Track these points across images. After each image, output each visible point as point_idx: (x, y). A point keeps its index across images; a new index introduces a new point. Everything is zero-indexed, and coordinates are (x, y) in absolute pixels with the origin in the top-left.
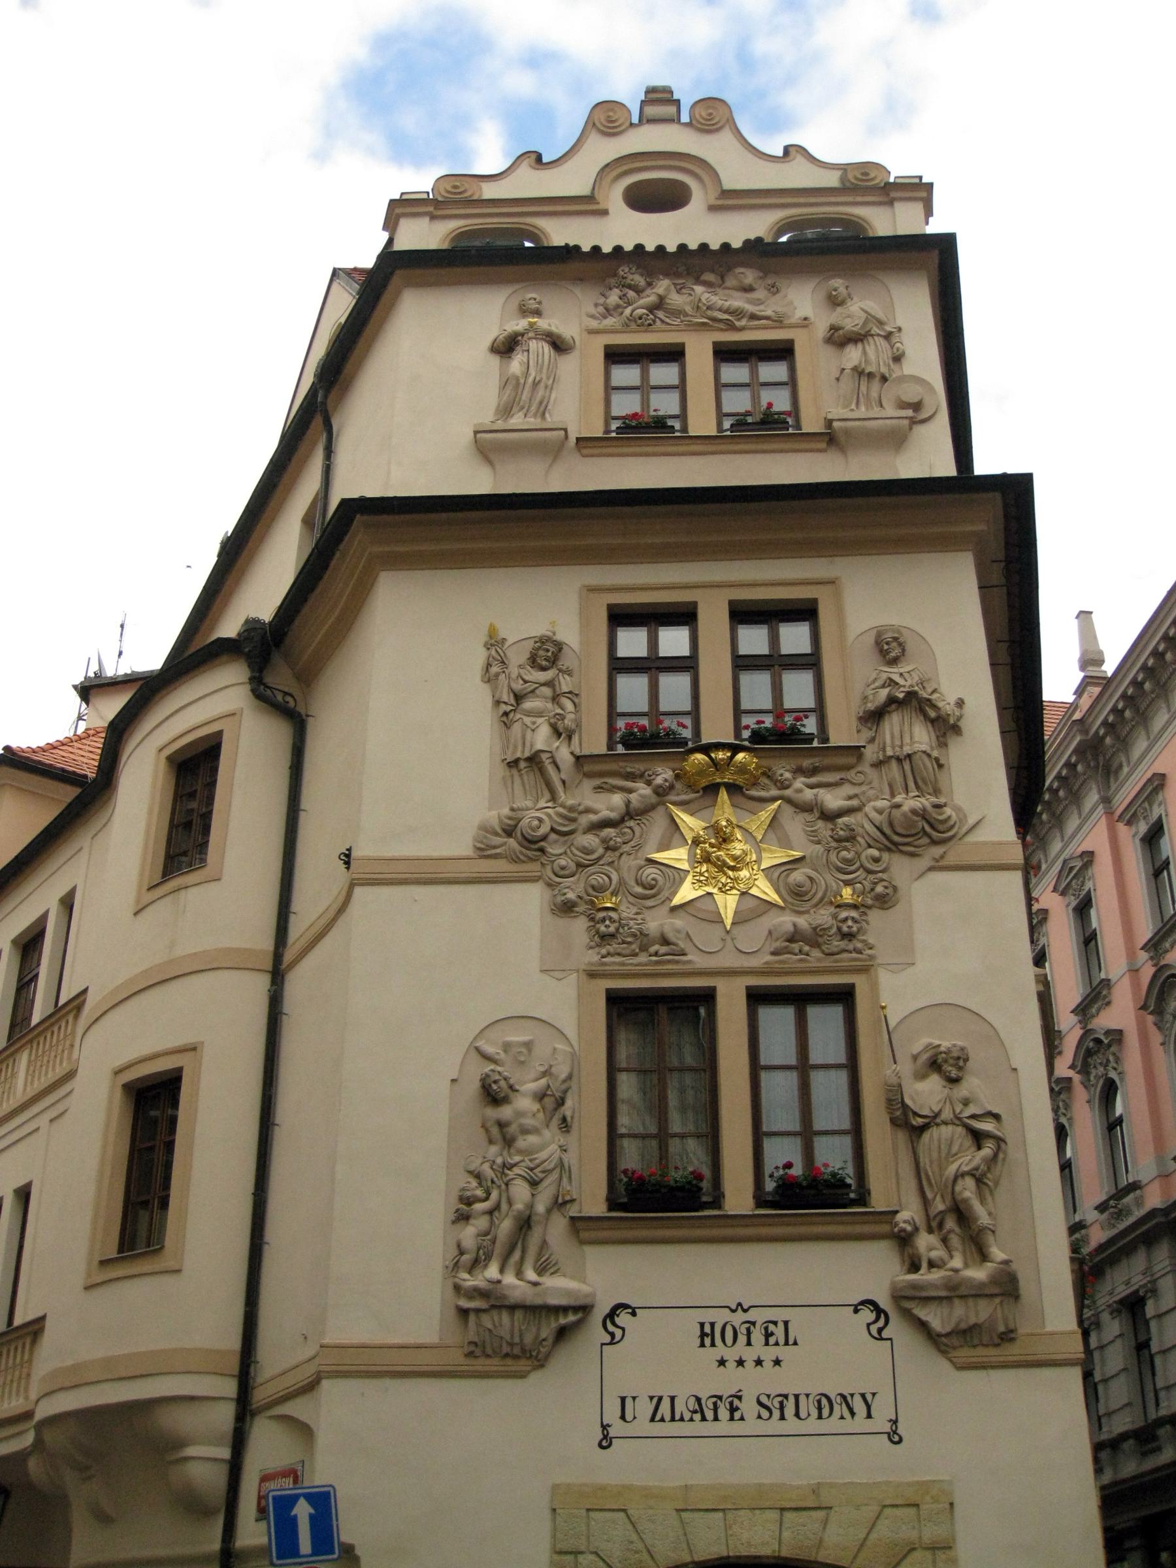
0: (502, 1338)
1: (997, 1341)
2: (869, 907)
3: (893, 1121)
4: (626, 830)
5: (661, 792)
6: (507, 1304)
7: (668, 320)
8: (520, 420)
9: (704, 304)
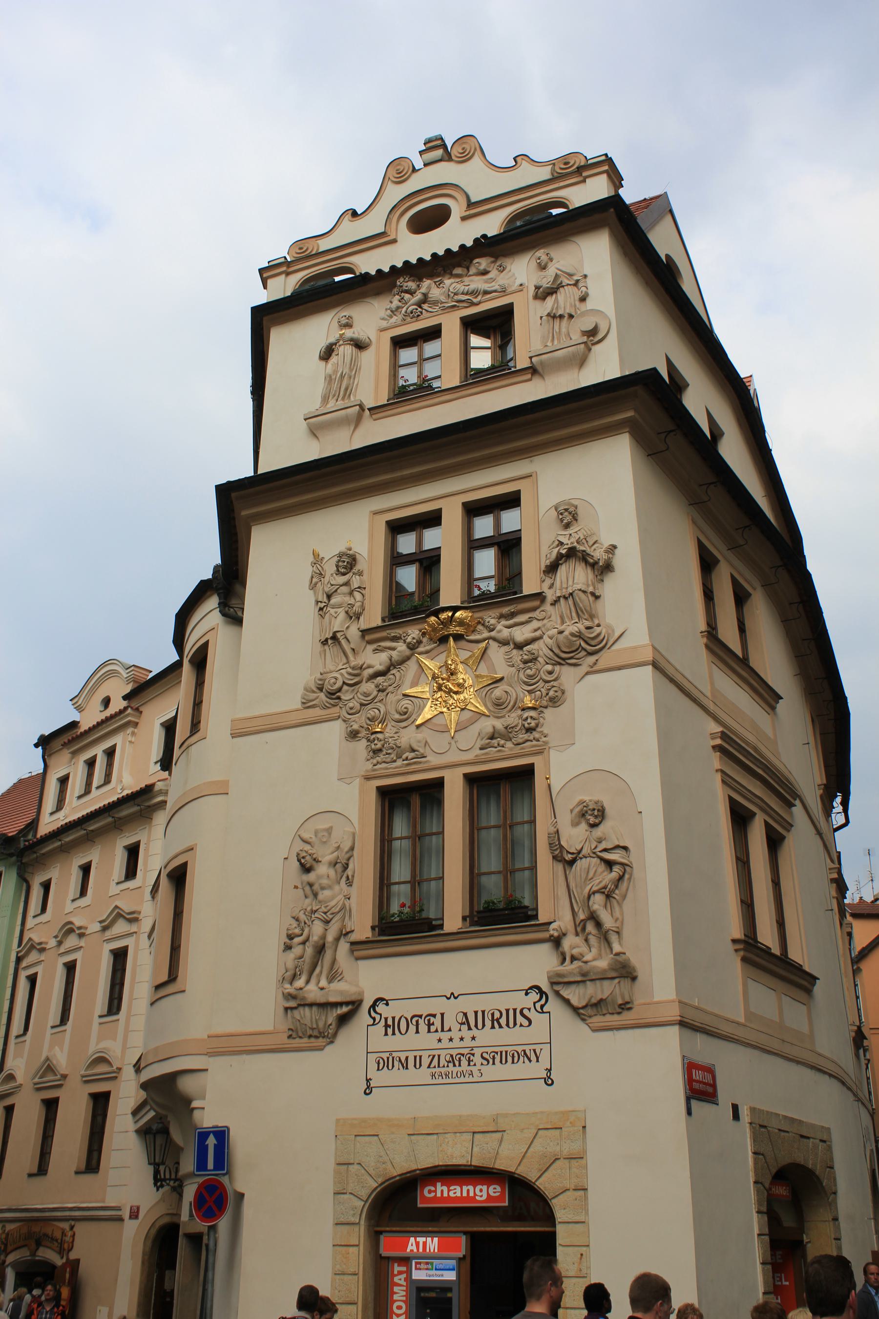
0: (306, 1025)
1: (620, 1010)
2: (546, 707)
3: (554, 858)
4: (392, 677)
5: (412, 647)
6: (307, 1003)
7: (430, 310)
8: (333, 405)
9: (452, 292)
